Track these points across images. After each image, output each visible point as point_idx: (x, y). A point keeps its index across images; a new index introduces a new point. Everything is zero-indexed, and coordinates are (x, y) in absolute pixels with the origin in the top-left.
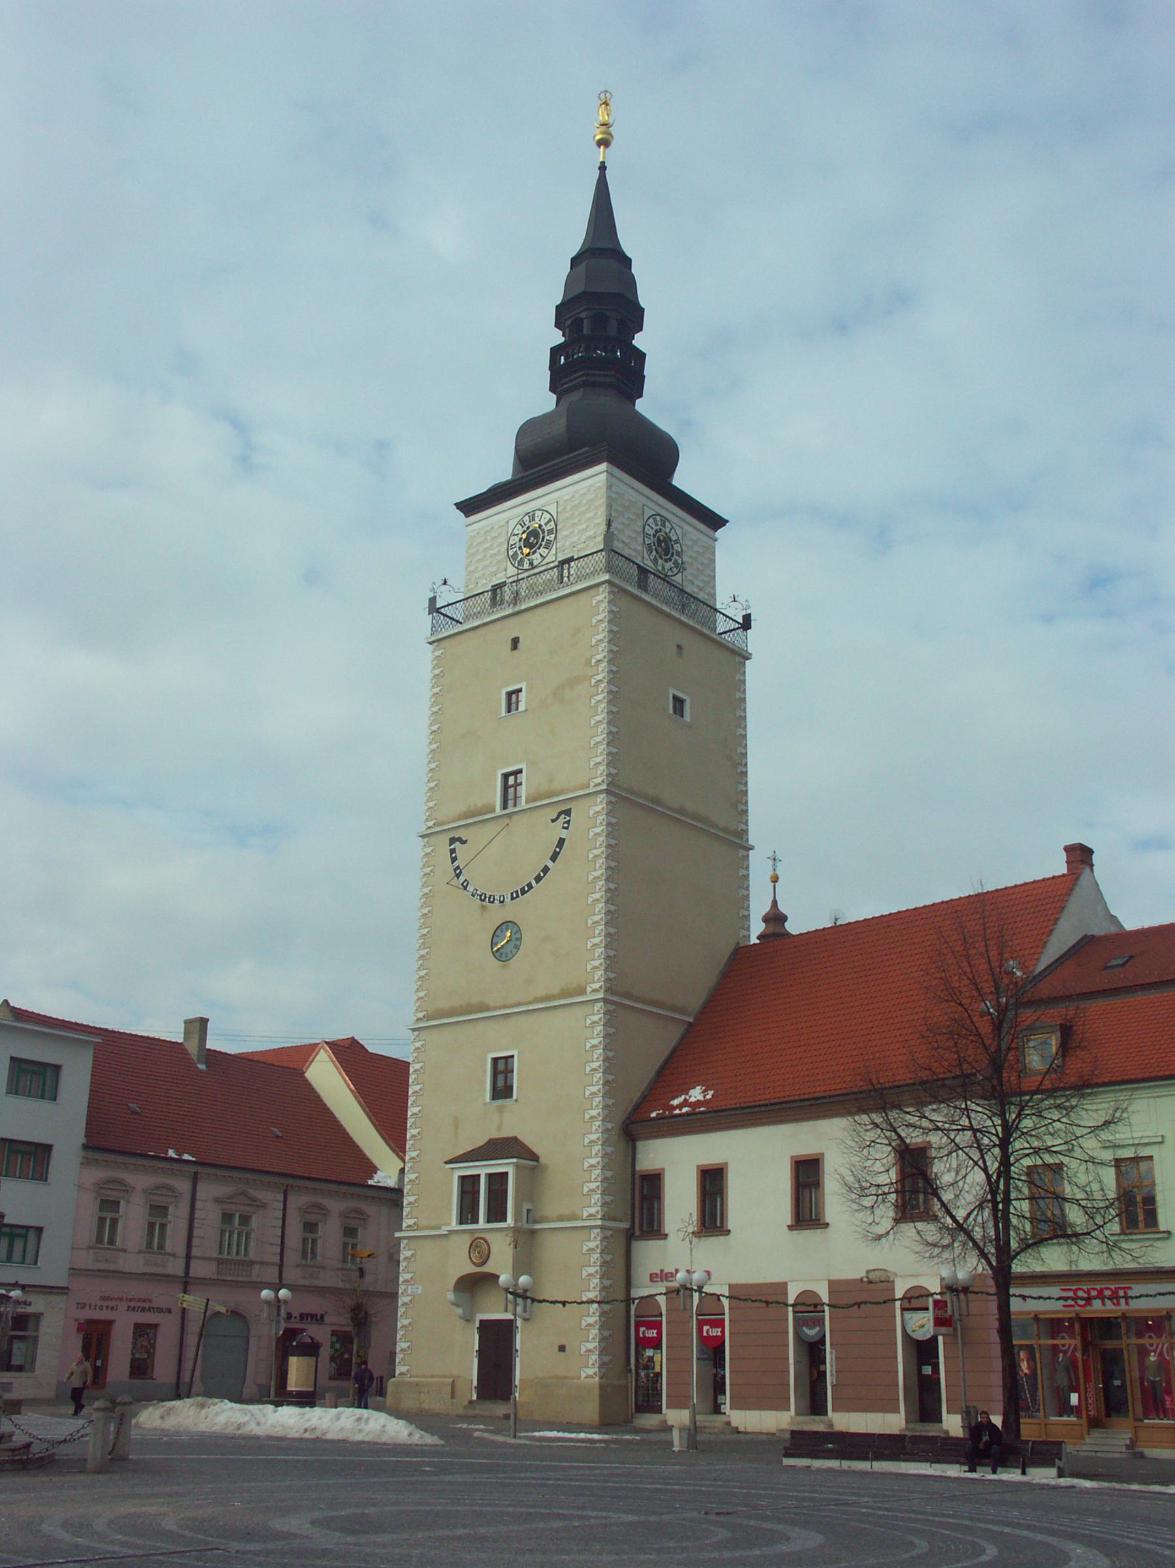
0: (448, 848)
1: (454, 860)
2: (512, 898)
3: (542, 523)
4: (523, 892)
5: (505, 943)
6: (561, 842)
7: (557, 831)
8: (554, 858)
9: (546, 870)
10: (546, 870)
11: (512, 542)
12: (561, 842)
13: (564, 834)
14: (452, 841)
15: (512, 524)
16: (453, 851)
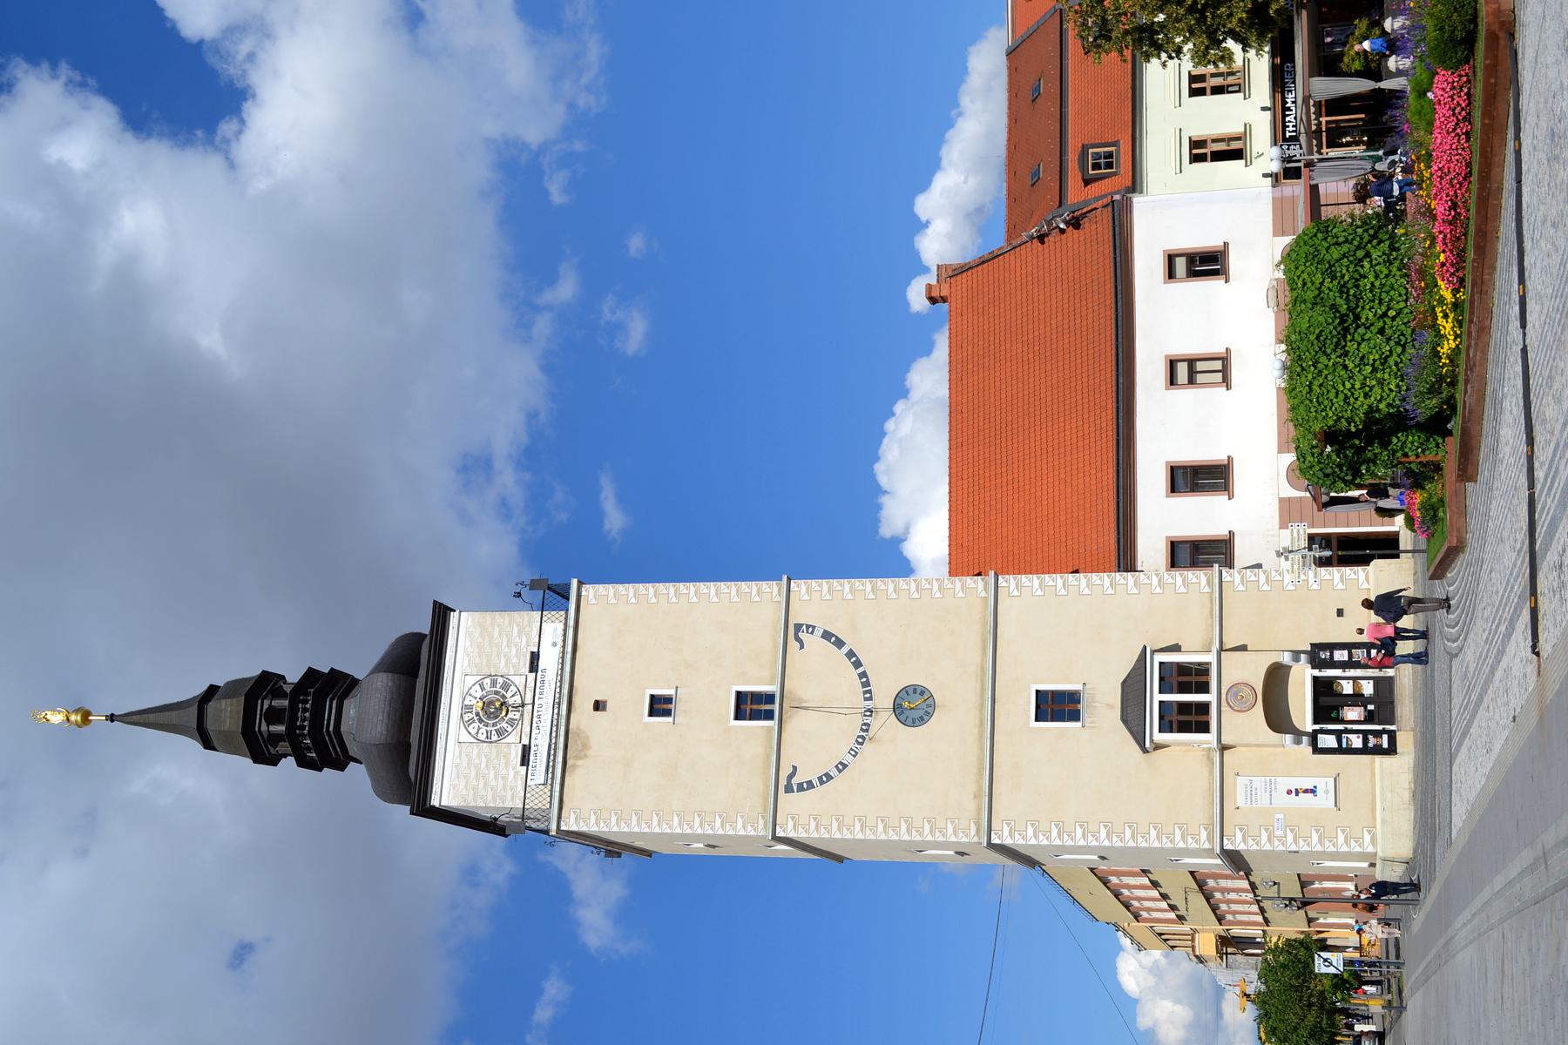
0: (796, 796)
2: (870, 699)
3: (479, 694)
4: (866, 684)
5: (913, 706)
6: (827, 635)
8: (839, 643)
9: (851, 654)
11: (483, 737)
12: (827, 635)
14: (789, 789)
15: (465, 737)
16: (801, 788)
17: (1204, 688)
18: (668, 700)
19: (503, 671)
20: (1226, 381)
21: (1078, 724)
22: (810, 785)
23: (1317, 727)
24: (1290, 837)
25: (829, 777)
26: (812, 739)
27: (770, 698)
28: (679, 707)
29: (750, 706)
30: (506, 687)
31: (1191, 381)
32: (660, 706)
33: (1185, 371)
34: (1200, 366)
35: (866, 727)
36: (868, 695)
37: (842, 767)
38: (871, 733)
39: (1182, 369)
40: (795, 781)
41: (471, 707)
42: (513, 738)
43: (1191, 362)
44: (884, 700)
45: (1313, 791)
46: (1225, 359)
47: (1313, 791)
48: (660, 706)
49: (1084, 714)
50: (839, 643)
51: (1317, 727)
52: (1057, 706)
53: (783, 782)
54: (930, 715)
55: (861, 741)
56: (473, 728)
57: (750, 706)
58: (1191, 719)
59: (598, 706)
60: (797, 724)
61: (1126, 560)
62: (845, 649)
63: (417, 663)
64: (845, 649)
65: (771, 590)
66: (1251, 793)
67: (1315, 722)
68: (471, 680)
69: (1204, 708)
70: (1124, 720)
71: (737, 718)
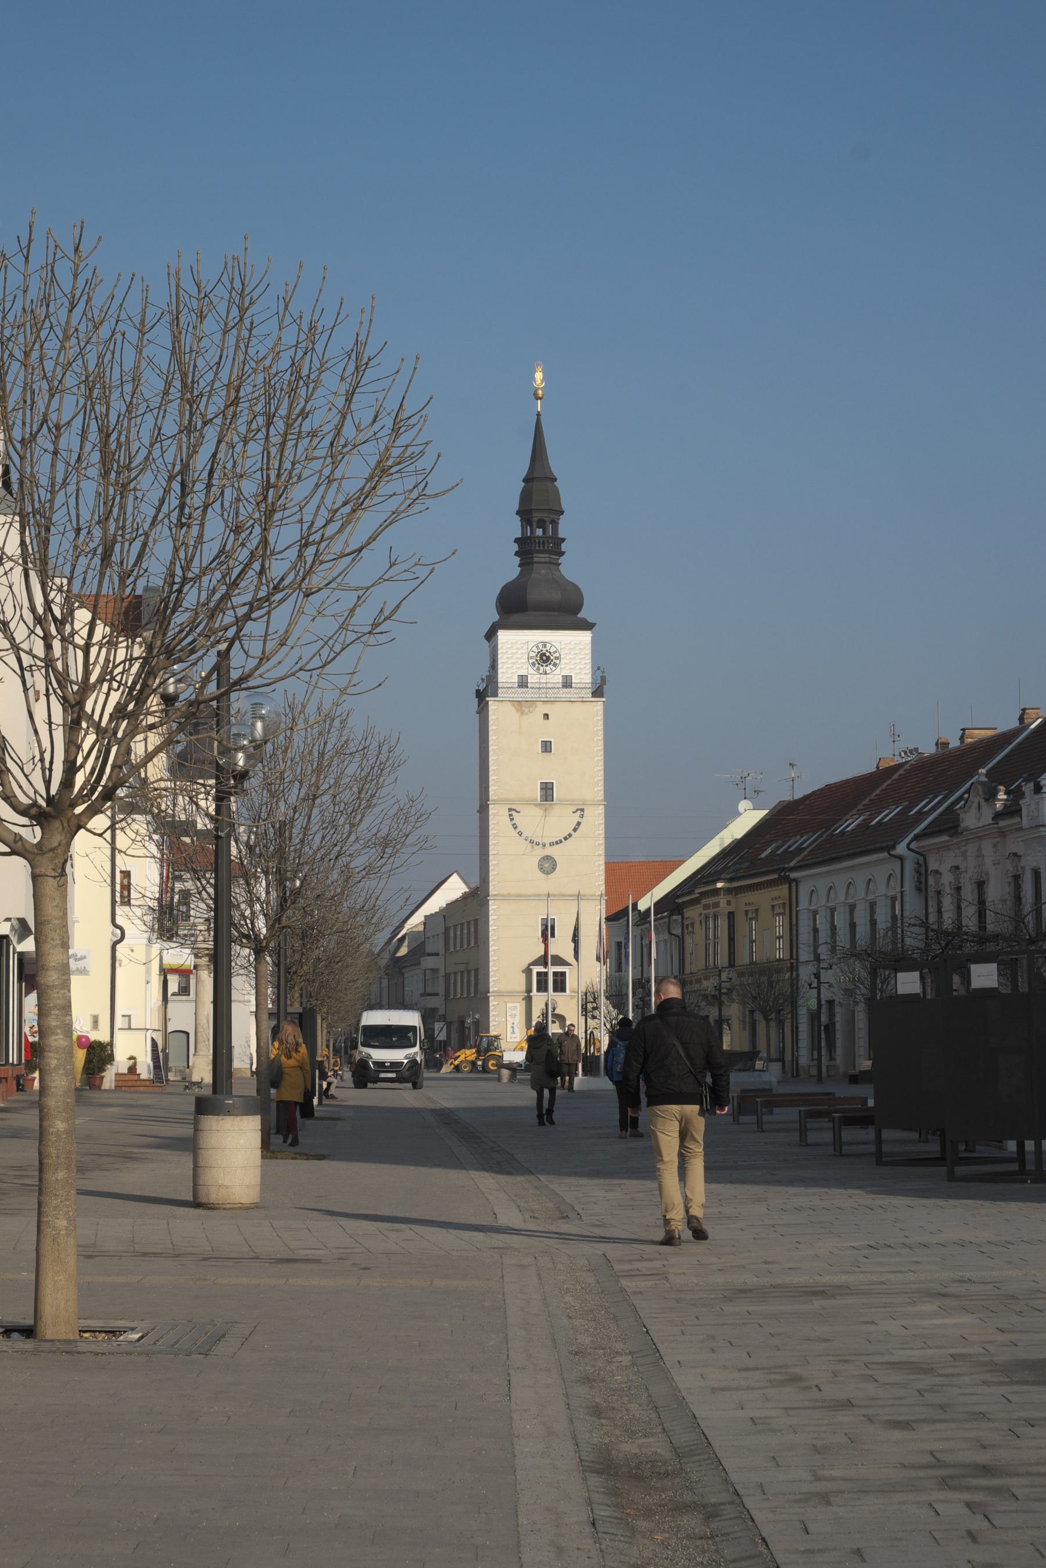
4: (557, 843)
5: (548, 865)
6: (579, 824)
7: (576, 818)
8: (575, 830)
9: (570, 835)
10: (570, 835)
12: (579, 824)
13: (580, 820)
14: (510, 810)
15: (531, 645)
16: (511, 815)
17: (555, 990)
19: (562, 662)
22: (512, 820)
25: (515, 828)
26: (530, 819)
29: (547, 789)
30: (555, 665)
32: (547, 747)
35: (538, 844)
36: (551, 844)
37: (520, 834)
38: (536, 847)
40: (513, 813)
41: (545, 646)
42: (531, 671)
48: (547, 747)
50: (575, 830)
55: (532, 842)
57: (547, 789)
58: (542, 987)
60: (539, 812)
63: (565, 612)
65: (601, 796)
69: (546, 990)
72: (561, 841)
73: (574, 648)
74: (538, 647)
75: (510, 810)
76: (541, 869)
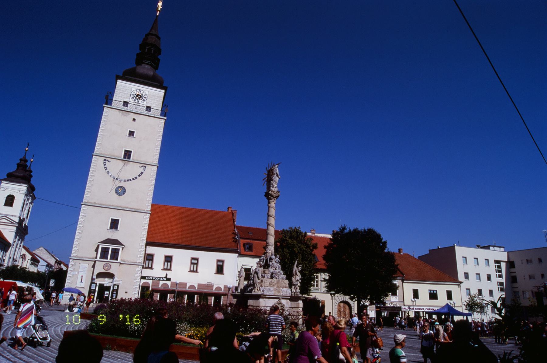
0: (103, 161)
1: (105, 165)
4: (128, 181)
5: (121, 191)
6: (142, 173)
7: (141, 170)
8: (139, 176)
12: (142, 173)
13: (143, 171)
15: (133, 89)
16: (104, 163)
18: (133, 135)
20: (191, 271)
21: (109, 228)
23: (98, 284)
24: (71, 275)
27: (129, 158)
28: (130, 138)
29: (128, 154)
30: (144, 100)
31: (192, 263)
32: (131, 133)
33: (195, 262)
34: (195, 266)
39: (196, 262)
40: (106, 162)
43: (197, 264)
44: (122, 184)
45: (81, 282)
46: (196, 271)
47: (81, 282)
48: (131, 133)
49: (111, 230)
50: (139, 176)
51: (98, 284)
52: (114, 224)
53: (107, 159)
54: (118, 194)
56: (135, 91)
57: (128, 154)
59: (134, 120)
60: (121, 163)
61: (149, 243)
62: (138, 177)
64: (138, 177)
65: (156, 161)
66: (83, 267)
67: (100, 284)
68: (147, 93)
70: (108, 239)
71: (125, 151)
72: (130, 180)
73: (155, 96)
74: (136, 91)
75: (105, 160)
76: (117, 191)
